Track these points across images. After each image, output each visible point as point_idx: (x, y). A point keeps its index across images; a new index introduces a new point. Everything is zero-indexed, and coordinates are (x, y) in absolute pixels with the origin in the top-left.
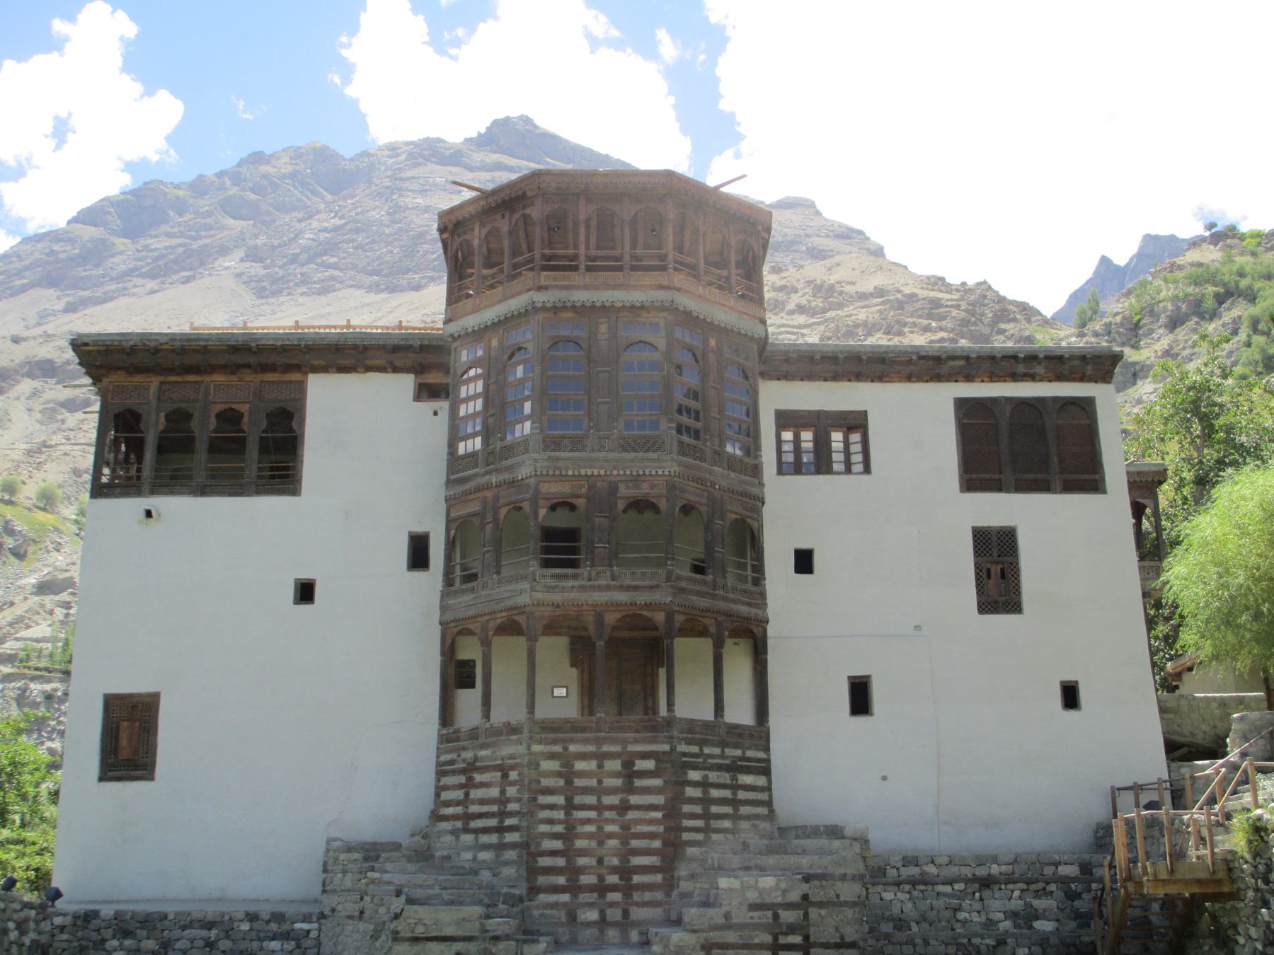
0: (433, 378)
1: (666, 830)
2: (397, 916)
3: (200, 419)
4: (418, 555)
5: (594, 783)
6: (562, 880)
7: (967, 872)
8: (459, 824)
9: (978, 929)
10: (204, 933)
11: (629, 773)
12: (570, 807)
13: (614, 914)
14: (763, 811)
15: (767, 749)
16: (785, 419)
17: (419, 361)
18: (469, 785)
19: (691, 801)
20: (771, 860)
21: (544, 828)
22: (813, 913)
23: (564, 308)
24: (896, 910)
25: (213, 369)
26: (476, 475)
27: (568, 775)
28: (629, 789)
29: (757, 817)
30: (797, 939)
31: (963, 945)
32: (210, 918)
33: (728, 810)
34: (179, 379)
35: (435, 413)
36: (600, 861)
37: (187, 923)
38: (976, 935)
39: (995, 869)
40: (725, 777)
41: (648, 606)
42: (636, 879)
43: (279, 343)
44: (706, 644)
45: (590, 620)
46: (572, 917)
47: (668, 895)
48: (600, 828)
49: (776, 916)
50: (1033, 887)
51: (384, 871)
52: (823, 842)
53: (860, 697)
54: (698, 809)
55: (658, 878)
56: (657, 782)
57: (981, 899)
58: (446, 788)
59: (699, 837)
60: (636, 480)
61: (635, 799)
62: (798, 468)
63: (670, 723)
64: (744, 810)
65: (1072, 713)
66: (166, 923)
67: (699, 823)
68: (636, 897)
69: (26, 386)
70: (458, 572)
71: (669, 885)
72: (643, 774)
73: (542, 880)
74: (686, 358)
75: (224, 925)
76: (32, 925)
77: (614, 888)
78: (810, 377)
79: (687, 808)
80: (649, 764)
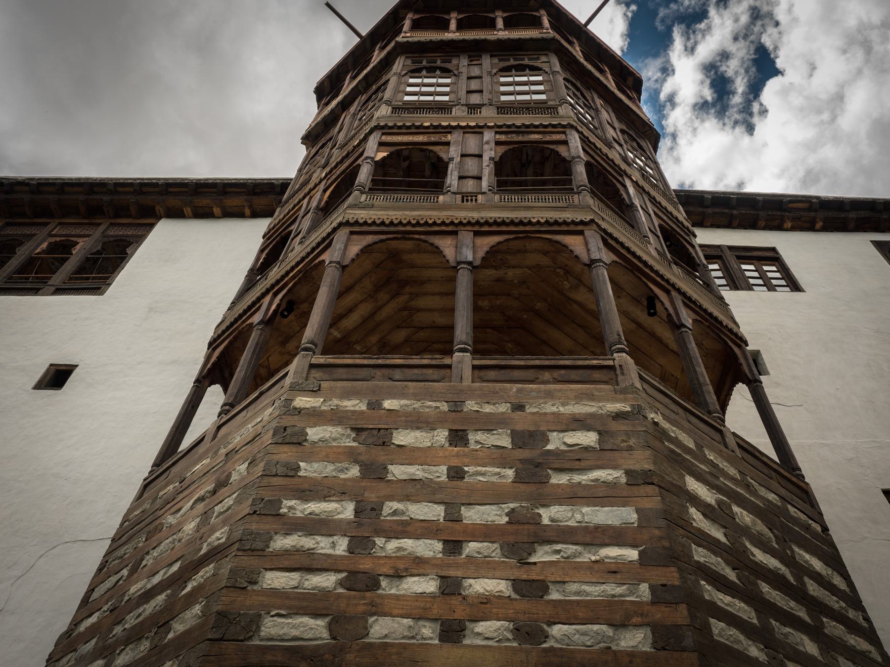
12: (367, 526)
48: (450, 587)
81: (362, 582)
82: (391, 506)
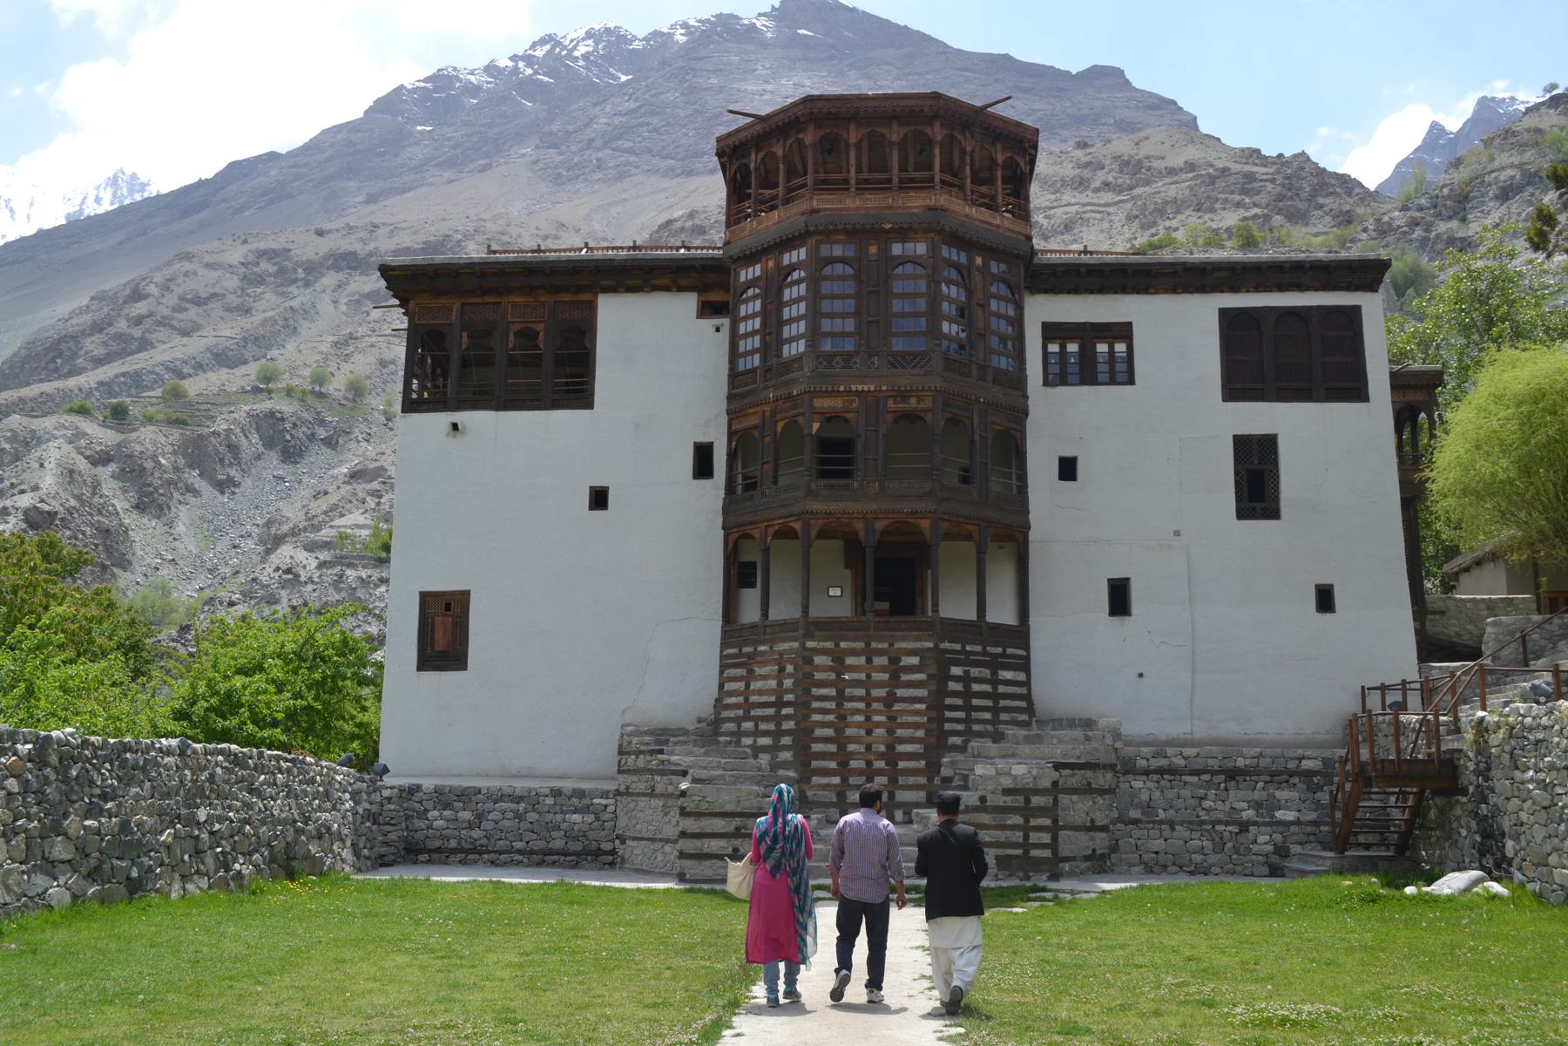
0: (714, 297)
2: (683, 794)
3: (496, 333)
4: (703, 463)
5: (863, 676)
6: (833, 765)
7: (1213, 764)
8: (741, 712)
9: (1221, 816)
10: (513, 806)
11: (895, 669)
12: (840, 698)
14: (1023, 704)
15: (1027, 648)
16: (1052, 331)
17: (704, 280)
18: (750, 676)
19: (955, 694)
20: (1026, 749)
21: (816, 717)
22: (1064, 799)
24: (1144, 797)
25: (509, 291)
26: (754, 391)
27: (839, 666)
30: (1046, 822)
32: (518, 793)
33: (989, 703)
34: (479, 300)
35: (718, 330)
36: (868, 748)
37: (500, 797)
38: (1220, 822)
39: (1241, 762)
40: (986, 673)
41: (914, 513)
42: (902, 764)
44: (969, 547)
45: (859, 526)
47: (930, 780)
48: (868, 718)
49: (1028, 801)
50: (1277, 779)
51: (672, 753)
52: (1078, 733)
53: (1119, 598)
54: (959, 702)
56: (921, 677)
57: (1226, 789)
58: (731, 679)
59: (961, 727)
60: (903, 395)
61: (900, 692)
62: (1063, 380)
63: (931, 625)
64: (1003, 703)
65: (1329, 616)
67: (961, 715)
68: (901, 780)
69: (330, 279)
70: (740, 480)
71: (933, 768)
72: (910, 669)
73: (814, 764)
74: (954, 274)
75: (531, 799)
76: (364, 796)
77: (880, 772)
78: (1076, 290)
79: (948, 701)
80: (915, 660)
81: (842, 718)
82: (848, 691)
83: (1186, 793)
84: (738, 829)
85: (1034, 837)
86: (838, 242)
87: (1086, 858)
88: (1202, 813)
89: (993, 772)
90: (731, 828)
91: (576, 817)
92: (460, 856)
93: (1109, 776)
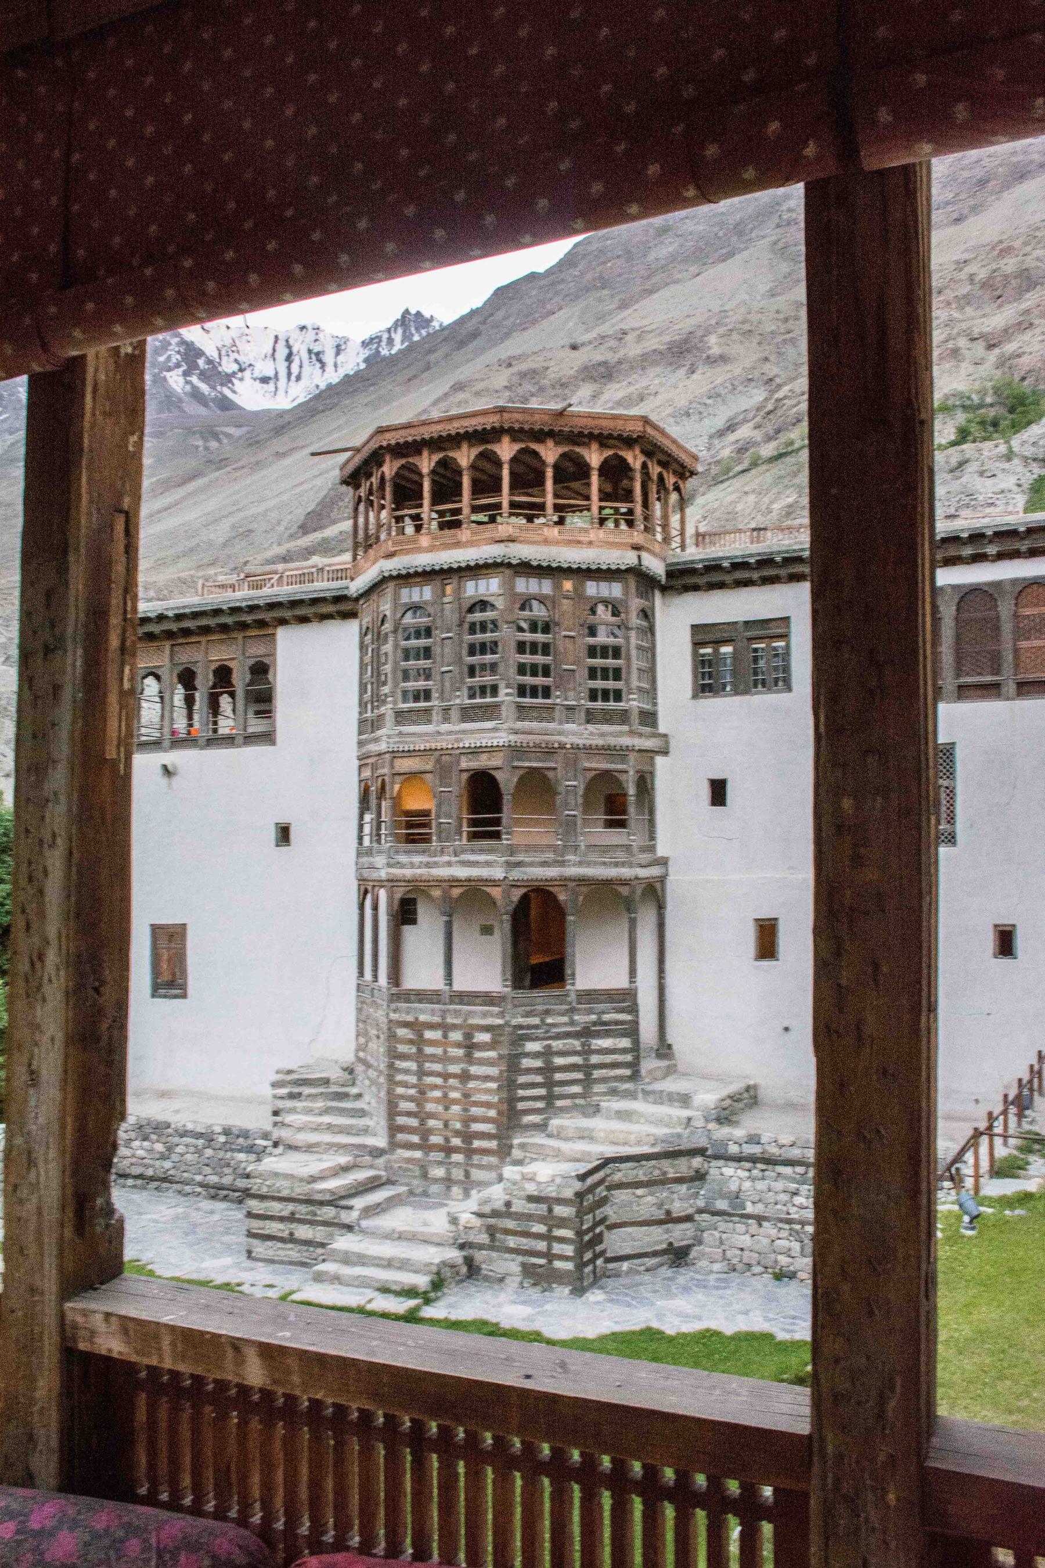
1: (500, 1100)
5: (439, 1051)
6: (415, 1139)
11: (470, 1047)
12: (421, 1073)
13: (458, 1174)
14: (628, 1072)
16: (703, 635)
19: (529, 1071)
21: (400, 1090)
23: (409, 576)
24: (733, 1187)
25: (206, 630)
27: (420, 1042)
28: (469, 1058)
29: (617, 1078)
31: (797, 1232)
33: (580, 1076)
37: (184, 1134)
40: (576, 1044)
42: (477, 1144)
43: (244, 604)
46: (425, 1176)
48: (445, 1095)
49: (550, 1210)
54: (539, 1079)
55: (493, 1144)
56: (492, 1054)
59: (540, 1105)
60: (475, 752)
61: (474, 1070)
64: (597, 1074)
66: (170, 1130)
67: (542, 1092)
68: (476, 1159)
71: (504, 1151)
73: (400, 1137)
75: (208, 1138)
79: (522, 1079)
80: (484, 1037)
81: (422, 1092)
82: (427, 1065)
83: (779, 1185)
84: (293, 1213)
85: (557, 1248)
86: (416, 584)
87: (655, 1254)
88: (793, 1210)
89: (518, 1177)
90: (285, 1213)
91: (241, 1156)
92: (156, 1184)
93: (697, 1162)
